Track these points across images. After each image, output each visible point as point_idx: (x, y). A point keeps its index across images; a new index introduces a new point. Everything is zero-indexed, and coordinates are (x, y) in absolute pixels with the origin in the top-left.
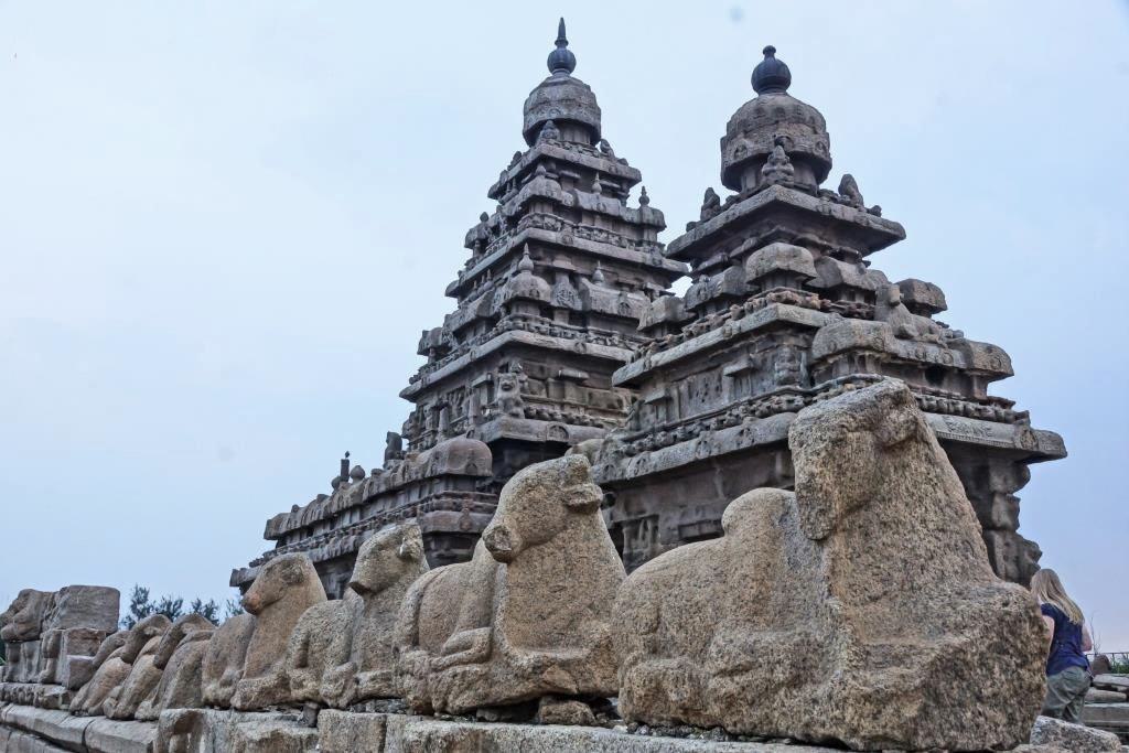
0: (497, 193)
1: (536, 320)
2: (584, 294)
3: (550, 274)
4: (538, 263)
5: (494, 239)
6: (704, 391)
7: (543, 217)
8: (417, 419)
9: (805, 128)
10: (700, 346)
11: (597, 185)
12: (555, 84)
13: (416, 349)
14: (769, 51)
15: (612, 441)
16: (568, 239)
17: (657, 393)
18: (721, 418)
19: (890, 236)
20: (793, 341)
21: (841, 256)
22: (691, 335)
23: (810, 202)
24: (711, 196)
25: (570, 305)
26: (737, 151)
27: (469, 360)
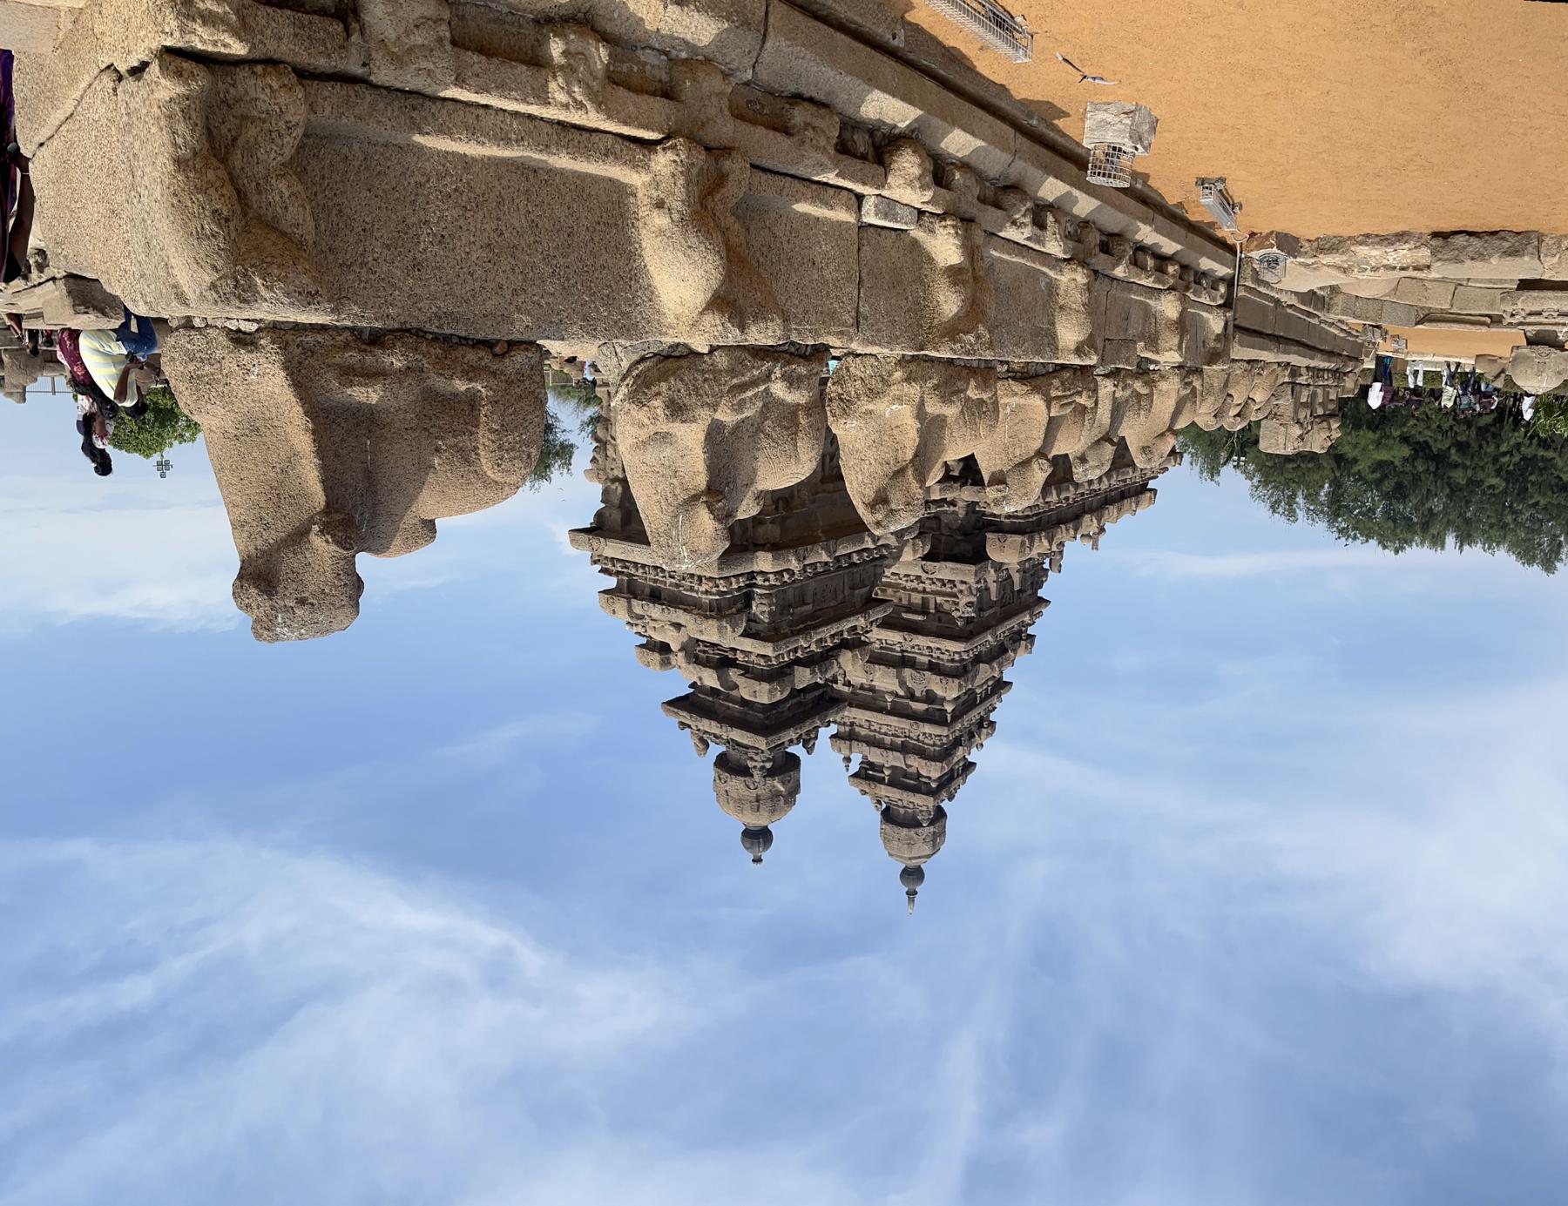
0: (969, 766)
1: (942, 660)
2: (902, 684)
3: (930, 697)
4: (940, 707)
7: (934, 745)
8: (1037, 583)
9: (736, 796)
11: (887, 772)
16: (915, 727)
20: (760, 627)
21: (714, 691)
23: (738, 735)
24: (809, 744)
25: (914, 672)
26: (789, 781)
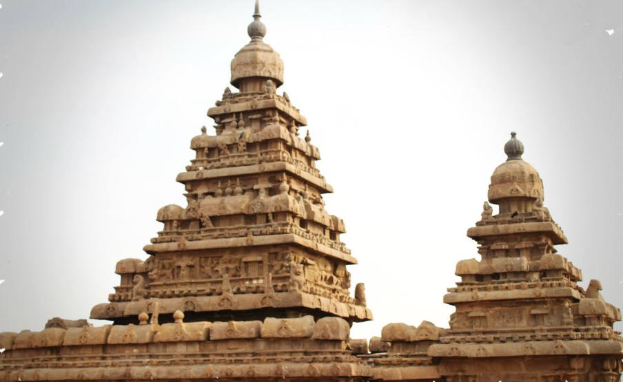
2: (307, 207)
5: (228, 152)
6: (509, 317)
7: (283, 153)
8: (158, 268)
10: (515, 297)
12: (265, 51)
13: (155, 217)
14: (513, 135)
15: (426, 328)
17: (476, 312)
18: (532, 334)
19: (561, 241)
22: (507, 288)
24: (487, 210)
27: (245, 244)
